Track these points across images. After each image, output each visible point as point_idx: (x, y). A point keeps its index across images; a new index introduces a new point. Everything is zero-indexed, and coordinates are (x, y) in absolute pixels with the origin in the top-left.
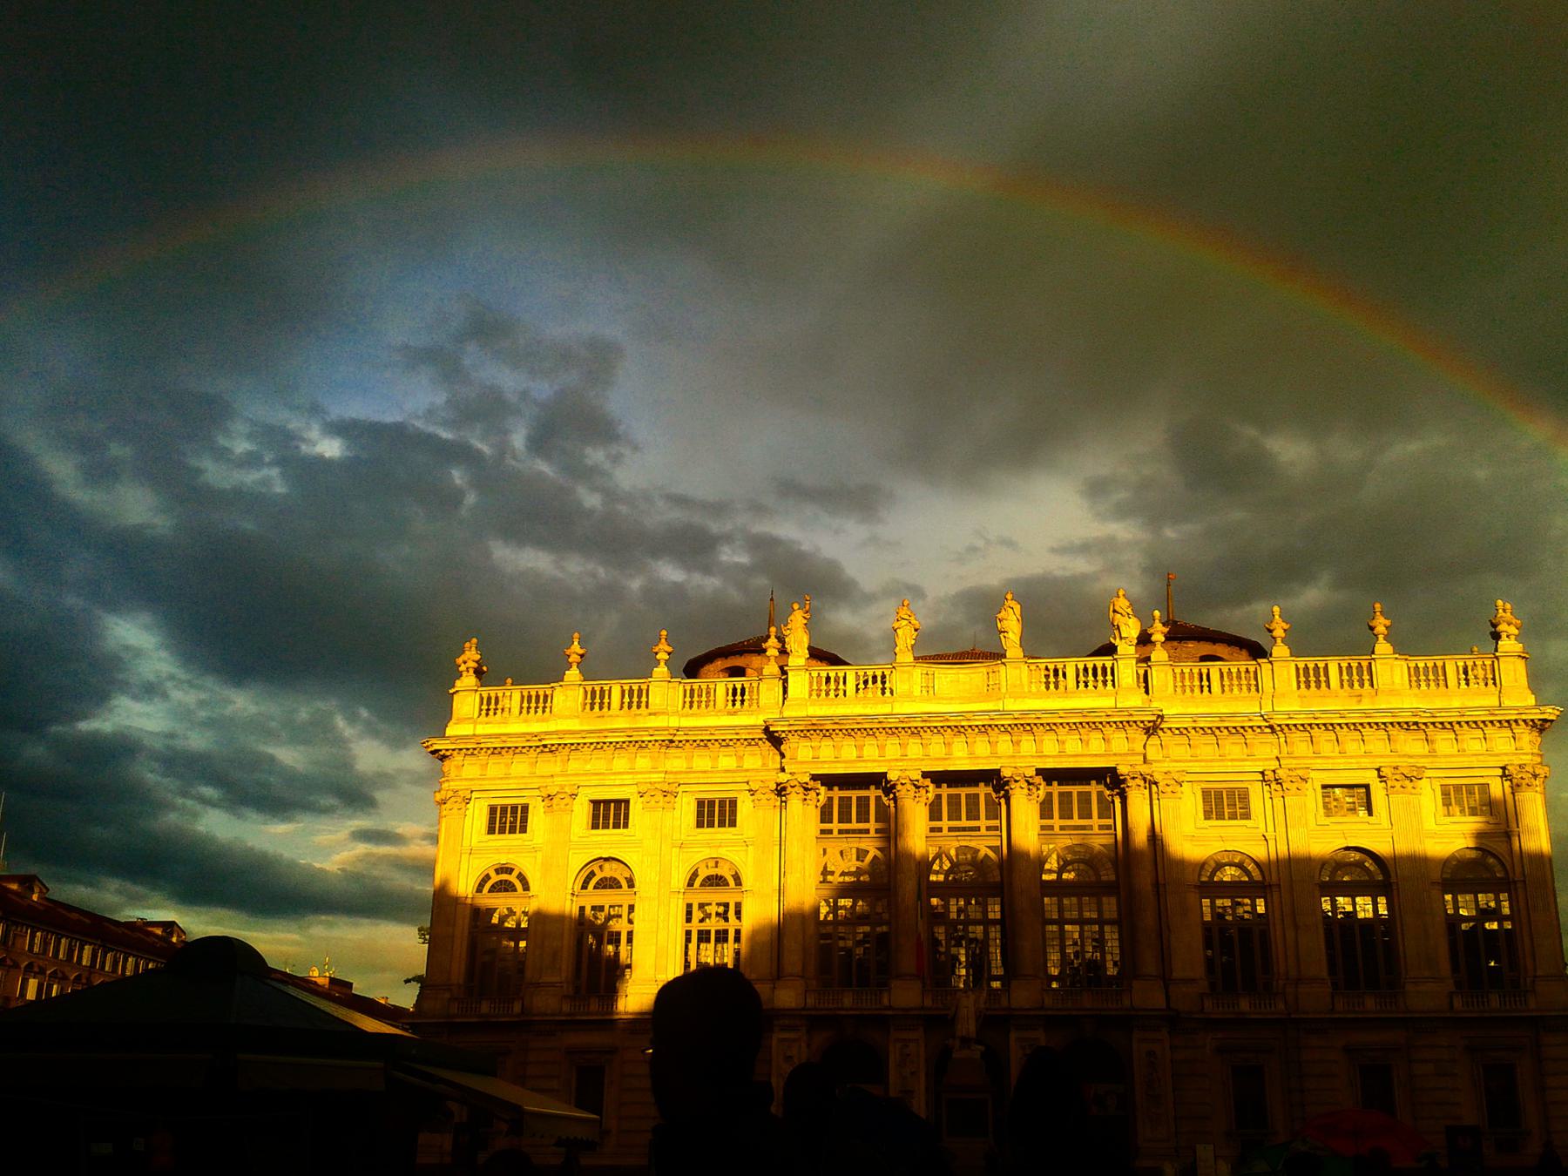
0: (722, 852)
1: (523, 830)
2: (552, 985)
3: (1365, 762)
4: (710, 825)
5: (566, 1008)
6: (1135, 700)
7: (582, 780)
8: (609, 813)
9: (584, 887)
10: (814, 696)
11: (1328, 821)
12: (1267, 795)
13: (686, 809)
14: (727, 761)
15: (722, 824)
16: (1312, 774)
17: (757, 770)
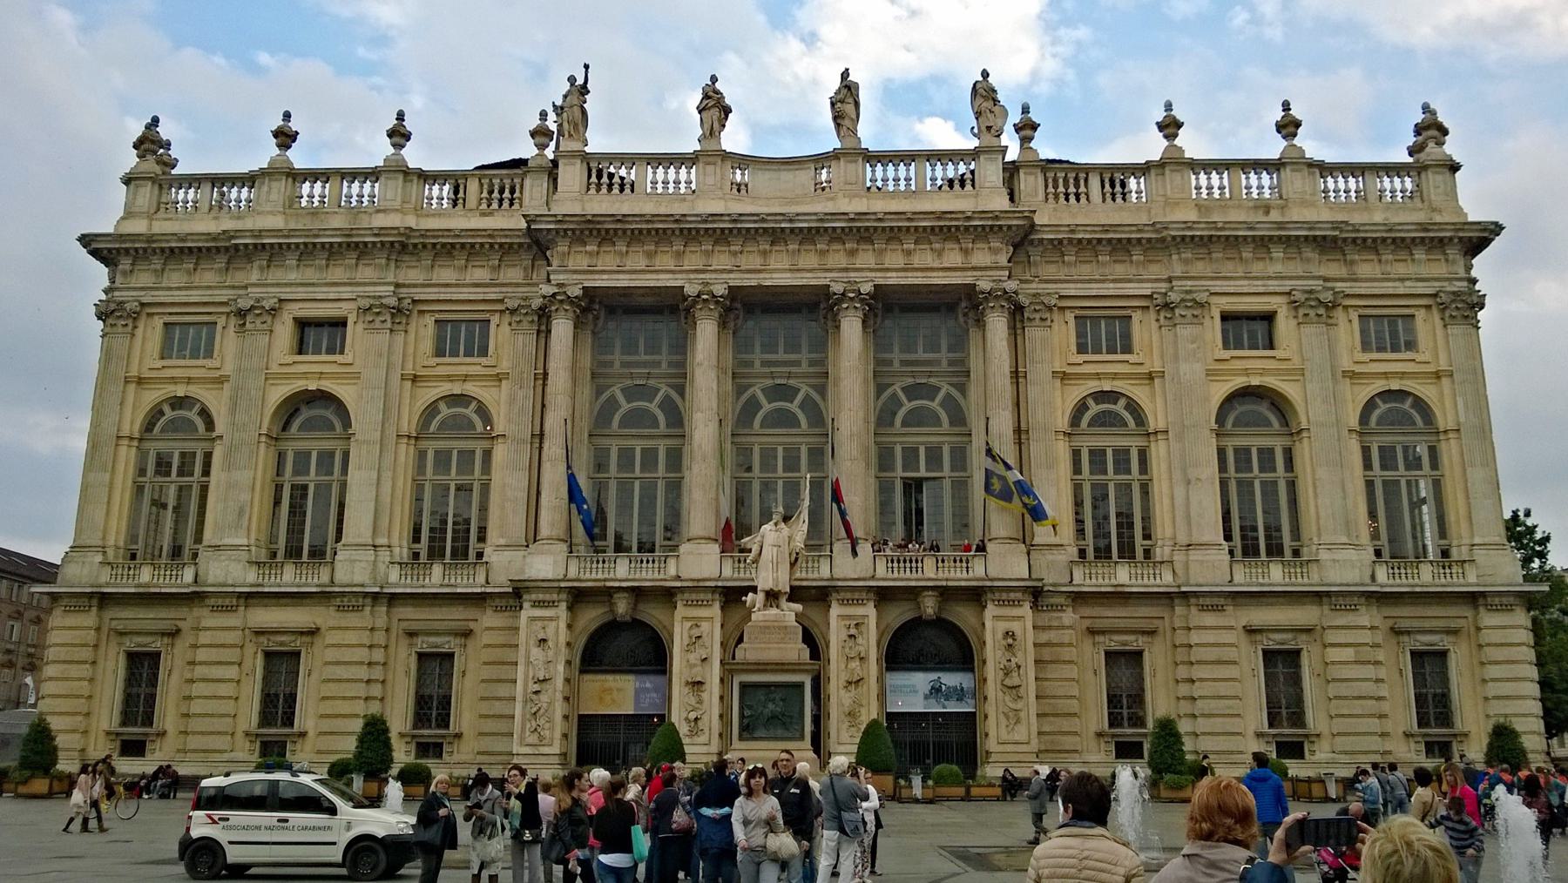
0: (471, 389)
1: (209, 354)
2: (236, 547)
3: (1273, 285)
4: (454, 354)
5: (252, 576)
6: (1000, 202)
7: (286, 293)
8: (321, 333)
9: (284, 429)
10: (593, 191)
11: (1227, 354)
12: (1155, 325)
13: (424, 330)
14: (480, 274)
15: (468, 354)
16: (1214, 300)
17: (517, 285)
